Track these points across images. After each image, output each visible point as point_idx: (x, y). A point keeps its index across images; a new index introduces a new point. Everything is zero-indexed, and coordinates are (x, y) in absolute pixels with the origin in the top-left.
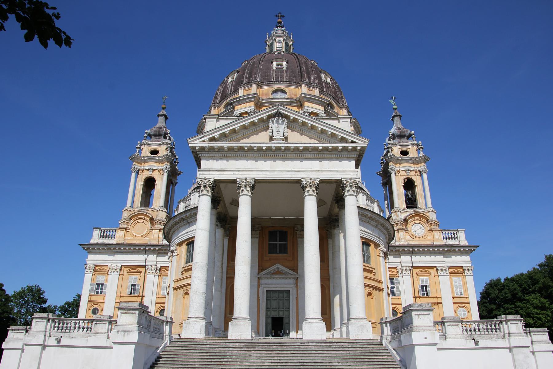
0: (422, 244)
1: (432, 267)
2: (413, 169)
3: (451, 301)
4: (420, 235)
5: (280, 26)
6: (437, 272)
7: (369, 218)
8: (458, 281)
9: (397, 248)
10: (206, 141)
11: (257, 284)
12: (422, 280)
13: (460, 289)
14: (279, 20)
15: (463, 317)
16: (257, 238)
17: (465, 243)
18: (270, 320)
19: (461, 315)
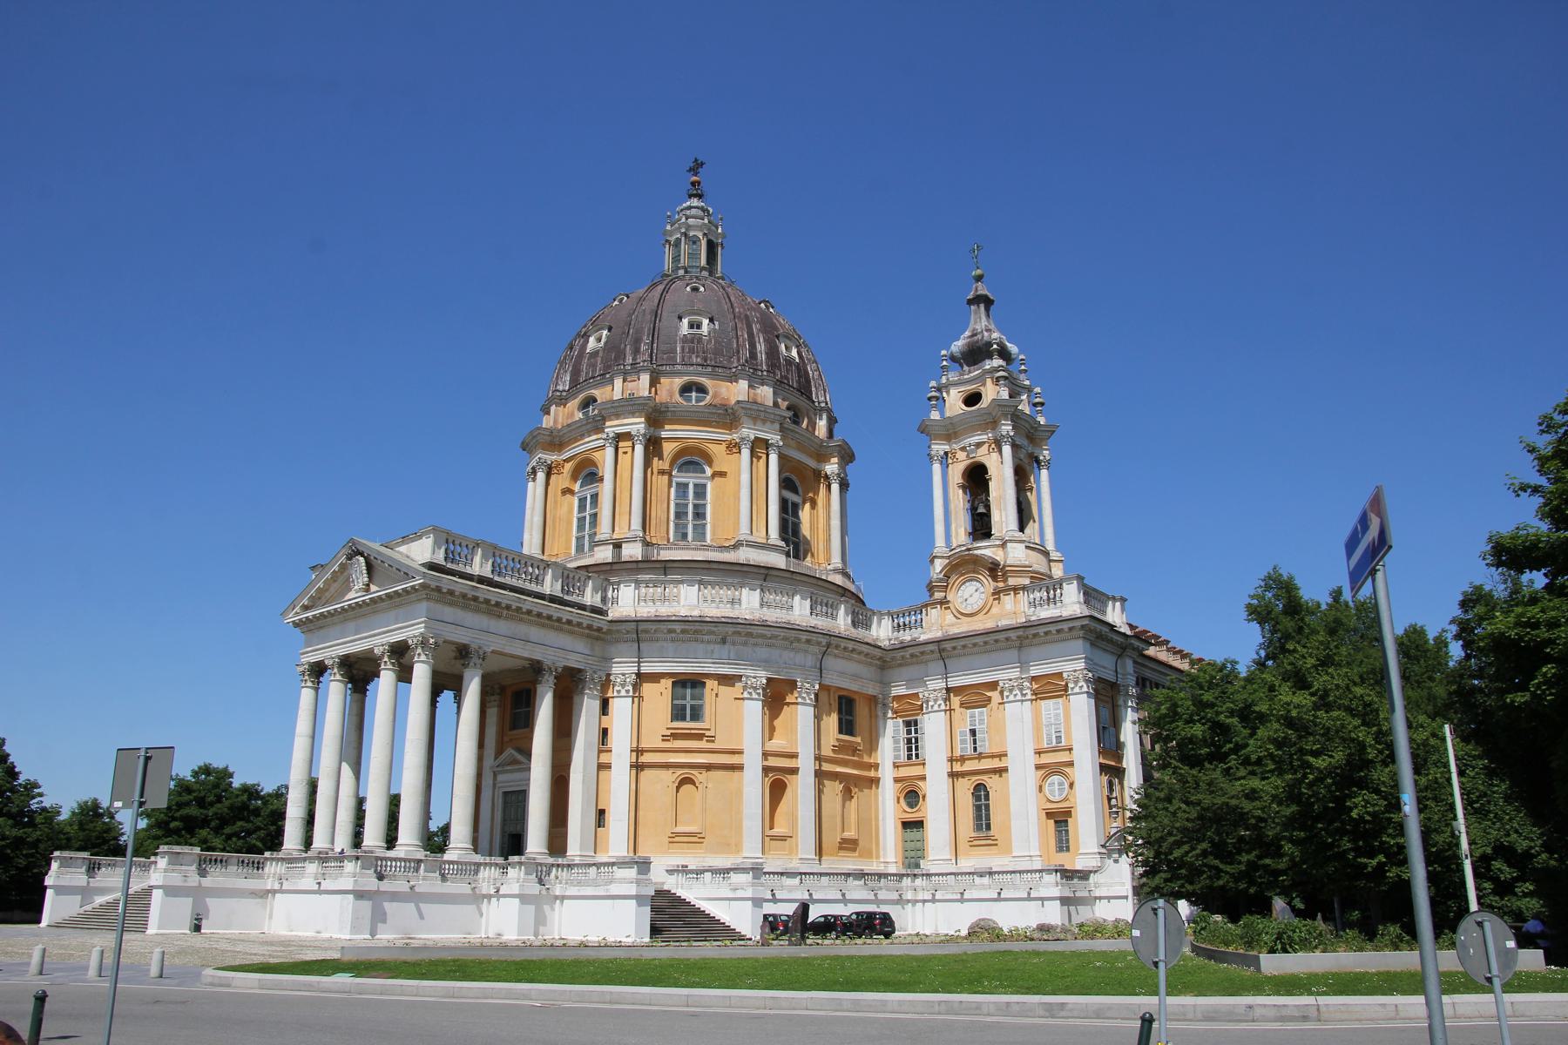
0: (975, 631)
1: (993, 685)
2: (984, 438)
3: (1032, 760)
4: (976, 608)
6: (1002, 693)
7: (683, 631)
8: (1055, 709)
9: (911, 651)
11: (491, 782)
12: (972, 716)
14: (695, 178)
15: (1057, 798)
17: (1075, 611)
18: (506, 839)
19: (1052, 792)
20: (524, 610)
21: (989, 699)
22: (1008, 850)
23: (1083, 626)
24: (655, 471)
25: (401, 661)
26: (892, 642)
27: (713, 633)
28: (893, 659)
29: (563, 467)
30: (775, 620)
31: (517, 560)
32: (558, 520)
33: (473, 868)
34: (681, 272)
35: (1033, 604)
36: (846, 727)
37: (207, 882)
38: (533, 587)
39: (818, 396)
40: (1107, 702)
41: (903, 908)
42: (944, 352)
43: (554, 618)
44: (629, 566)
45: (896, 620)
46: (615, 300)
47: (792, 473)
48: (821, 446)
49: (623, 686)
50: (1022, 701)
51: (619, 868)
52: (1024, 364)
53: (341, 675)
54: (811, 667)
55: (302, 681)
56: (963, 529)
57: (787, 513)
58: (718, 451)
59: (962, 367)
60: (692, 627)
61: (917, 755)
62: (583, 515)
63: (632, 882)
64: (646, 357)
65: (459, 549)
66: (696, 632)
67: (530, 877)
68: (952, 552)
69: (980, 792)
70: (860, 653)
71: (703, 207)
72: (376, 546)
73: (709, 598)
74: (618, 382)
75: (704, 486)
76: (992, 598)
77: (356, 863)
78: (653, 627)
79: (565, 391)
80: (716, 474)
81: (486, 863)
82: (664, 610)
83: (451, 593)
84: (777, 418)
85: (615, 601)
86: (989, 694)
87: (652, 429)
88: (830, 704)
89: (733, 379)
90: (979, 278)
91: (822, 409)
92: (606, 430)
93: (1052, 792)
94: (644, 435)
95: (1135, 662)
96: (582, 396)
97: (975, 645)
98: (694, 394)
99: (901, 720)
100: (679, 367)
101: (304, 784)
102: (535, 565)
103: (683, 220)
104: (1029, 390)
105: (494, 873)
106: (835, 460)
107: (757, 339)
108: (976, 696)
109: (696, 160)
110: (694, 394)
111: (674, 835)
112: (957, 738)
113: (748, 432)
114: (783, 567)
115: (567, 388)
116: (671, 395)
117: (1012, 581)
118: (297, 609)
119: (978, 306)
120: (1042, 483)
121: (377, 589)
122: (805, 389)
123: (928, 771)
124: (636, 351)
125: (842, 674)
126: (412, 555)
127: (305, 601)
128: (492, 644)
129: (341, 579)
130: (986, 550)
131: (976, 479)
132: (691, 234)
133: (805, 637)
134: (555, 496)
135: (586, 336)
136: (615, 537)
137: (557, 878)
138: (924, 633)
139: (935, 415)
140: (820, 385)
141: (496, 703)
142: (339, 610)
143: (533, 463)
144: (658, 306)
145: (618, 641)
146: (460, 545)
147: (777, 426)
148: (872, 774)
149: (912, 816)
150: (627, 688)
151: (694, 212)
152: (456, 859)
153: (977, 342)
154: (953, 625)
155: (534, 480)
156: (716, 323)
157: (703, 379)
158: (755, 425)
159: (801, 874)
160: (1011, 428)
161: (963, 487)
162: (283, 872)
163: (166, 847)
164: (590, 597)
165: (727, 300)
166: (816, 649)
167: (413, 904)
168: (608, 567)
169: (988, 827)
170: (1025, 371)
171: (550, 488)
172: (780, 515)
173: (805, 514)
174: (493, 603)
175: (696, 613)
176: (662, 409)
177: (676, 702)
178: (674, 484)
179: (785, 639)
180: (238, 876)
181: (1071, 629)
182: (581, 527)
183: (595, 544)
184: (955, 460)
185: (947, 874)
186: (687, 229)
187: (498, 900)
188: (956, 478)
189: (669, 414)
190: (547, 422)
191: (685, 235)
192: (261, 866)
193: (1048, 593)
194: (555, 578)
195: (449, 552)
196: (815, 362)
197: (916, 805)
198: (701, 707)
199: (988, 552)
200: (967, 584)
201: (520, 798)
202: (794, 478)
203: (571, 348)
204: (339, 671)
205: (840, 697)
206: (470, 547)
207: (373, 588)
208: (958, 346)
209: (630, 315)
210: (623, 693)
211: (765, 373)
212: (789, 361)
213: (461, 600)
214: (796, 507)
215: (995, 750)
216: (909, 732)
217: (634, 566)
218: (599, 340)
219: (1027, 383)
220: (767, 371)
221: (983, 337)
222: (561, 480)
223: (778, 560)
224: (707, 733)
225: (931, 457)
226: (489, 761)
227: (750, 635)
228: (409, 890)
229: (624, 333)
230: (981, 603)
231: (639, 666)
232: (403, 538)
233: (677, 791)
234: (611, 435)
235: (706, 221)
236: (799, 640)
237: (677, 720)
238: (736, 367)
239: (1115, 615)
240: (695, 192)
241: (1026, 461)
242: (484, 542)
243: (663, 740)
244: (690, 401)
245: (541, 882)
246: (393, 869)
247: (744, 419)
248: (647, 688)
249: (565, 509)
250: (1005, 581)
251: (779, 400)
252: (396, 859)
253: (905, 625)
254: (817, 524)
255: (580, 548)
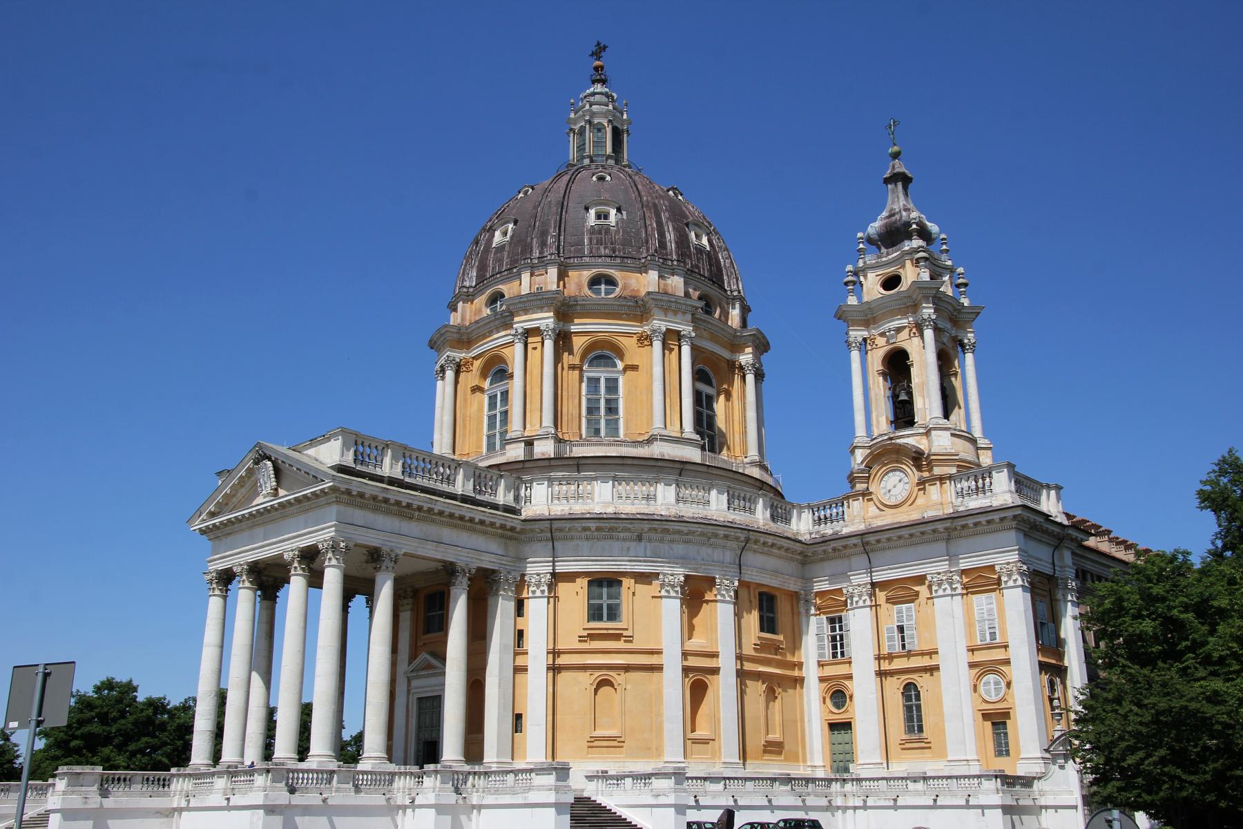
1: (921, 580)
3: (964, 658)
4: (900, 499)
5: (599, 81)
6: (930, 587)
7: (598, 529)
9: (833, 544)
10: (205, 518)
11: (406, 688)
12: (900, 612)
13: (990, 624)
14: (598, 63)
15: (994, 699)
16: (407, 610)
18: (421, 747)
19: (988, 692)
20: (436, 511)
21: (917, 594)
22: (942, 754)
23: (1015, 517)
24: (566, 366)
25: (311, 565)
26: (813, 536)
27: (628, 530)
28: (814, 553)
29: (472, 364)
30: (691, 515)
31: (427, 460)
32: (468, 418)
33: (387, 778)
34: (587, 162)
35: (960, 494)
36: (768, 624)
37: (109, 803)
38: (445, 487)
39: (730, 285)
40: (1045, 596)
41: (833, 816)
42: (860, 235)
43: (467, 518)
44: (541, 464)
45: (816, 513)
46: (519, 192)
47: (704, 364)
48: (735, 336)
49: (538, 586)
50: (952, 596)
51: (537, 775)
52: (945, 243)
53: (250, 582)
54: (730, 564)
55: (210, 589)
56: (884, 417)
57: (701, 406)
58: (628, 344)
59: (880, 249)
60: (607, 525)
61: (842, 654)
62: (493, 412)
63: (551, 790)
64: (554, 250)
65: (368, 451)
66: (611, 529)
67: (447, 786)
68: (874, 442)
69: (911, 692)
70: (780, 548)
71: (606, 93)
72: (283, 449)
73: (624, 495)
74: (526, 277)
75: (616, 380)
76: (917, 488)
77: (267, 776)
78: (568, 525)
79: (472, 287)
80: (628, 368)
81: (401, 773)
82: (578, 508)
83: (361, 495)
84: (689, 308)
85: (528, 499)
86: (916, 588)
87: (562, 323)
88: (751, 601)
89: (643, 269)
90: (896, 156)
91: (734, 298)
92: (514, 326)
93: (988, 692)
94: (554, 330)
95: (1073, 554)
96: (489, 292)
97: (900, 537)
98: (603, 287)
99: (824, 617)
100: (587, 259)
101: (213, 695)
102: (446, 465)
103: (587, 107)
104: (951, 270)
105: (409, 782)
106: (749, 350)
107: (666, 228)
108: (902, 591)
109: (599, 44)
110: (603, 287)
111: (593, 739)
112: (885, 635)
113: (660, 324)
114: (699, 461)
115: (474, 284)
116: (580, 287)
117: (937, 471)
118: (204, 516)
119: (896, 185)
120: (967, 368)
121: (285, 493)
122: (716, 278)
123: (855, 670)
124: (543, 244)
125: (763, 570)
126: (321, 458)
127: (212, 508)
128: (404, 546)
129: (249, 484)
130: (910, 439)
131: (897, 365)
132: (596, 121)
133: (722, 533)
134: (465, 394)
135: (492, 230)
136: (526, 434)
137: (474, 786)
138: (846, 526)
139: (852, 300)
140: (732, 273)
141: (409, 607)
142: (247, 516)
143: (442, 361)
144: (564, 197)
145: (531, 540)
146: (369, 446)
147: (689, 317)
148: (796, 673)
149: (839, 717)
150: (542, 588)
151: (598, 98)
152: (370, 770)
153: (895, 222)
154: (876, 517)
155: (443, 378)
156: (624, 213)
157: (612, 271)
158: (666, 317)
159: (725, 778)
160: (933, 311)
161: (884, 374)
162: (190, 788)
163: (65, 767)
164: (503, 496)
165: (635, 188)
166: (734, 544)
167: (326, 818)
168: (520, 466)
169: (921, 729)
170: (947, 251)
171: (459, 386)
172: (694, 408)
173: (720, 406)
174: (404, 504)
175: (610, 510)
176: (571, 303)
177: (592, 602)
178: (585, 379)
179: (702, 534)
180: (142, 794)
181: (1002, 519)
182: (492, 425)
183: (506, 442)
184: (874, 346)
185: (878, 779)
186: (591, 117)
187: (414, 811)
188: (875, 365)
189: (578, 307)
190: (455, 319)
191: (590, 122)
192: (167, 783)
193: (976, 482)
194: (466, 478)
195: (358, 453)
196: (726, 249)
197: (843, 706)
198: (618, 606)
199: (911, 441)
200: (891, 474)
201: (435, 704)
202: (707, 369)
203: (477, 242)
204: (248, 578)
205: (761, 594)
206: (380, 448)
207: (282, 492)
208: (874, 227)
209: (536, 208)
210: (538, 593)
211: (675, 263)
212: (700, 250)
213: (371, 502)
214: (710, 400)
215: (925, 647)
216: (833, 629)
217: (546, 463)
218: (505, 234)
219: (949, 263)
220: (678, 261)
221: (901, 217)
222: (470, 378)
223: (693, 454)
224: (625, 633)
225: (849, 344)
226: (403, 667)
227: (666, 531)
228: (322, 803)
229: (530, 226)
230: (905, 494)
231: (554, 566)
232: (311, 440)
233: (596, 694)
234: (520, 331)
235: (611, 107)
236: (716, 536)
237: (594, 620)
238: (646, 258)
239: (1050, 504)
240: (598, 77)
241: (950, 345)
242: (394, 443)
243: (580, 641)
244: (600, 293)
245: (457, 791)
246: (305, 781)
247: (655, 311)
248: (563, 588)
249: (475, 407)
250: (930, 470)
251: (691, 290)
252: (308, 771)
253: (826, 518)
254: (733, 416)
255: (491, 446)
